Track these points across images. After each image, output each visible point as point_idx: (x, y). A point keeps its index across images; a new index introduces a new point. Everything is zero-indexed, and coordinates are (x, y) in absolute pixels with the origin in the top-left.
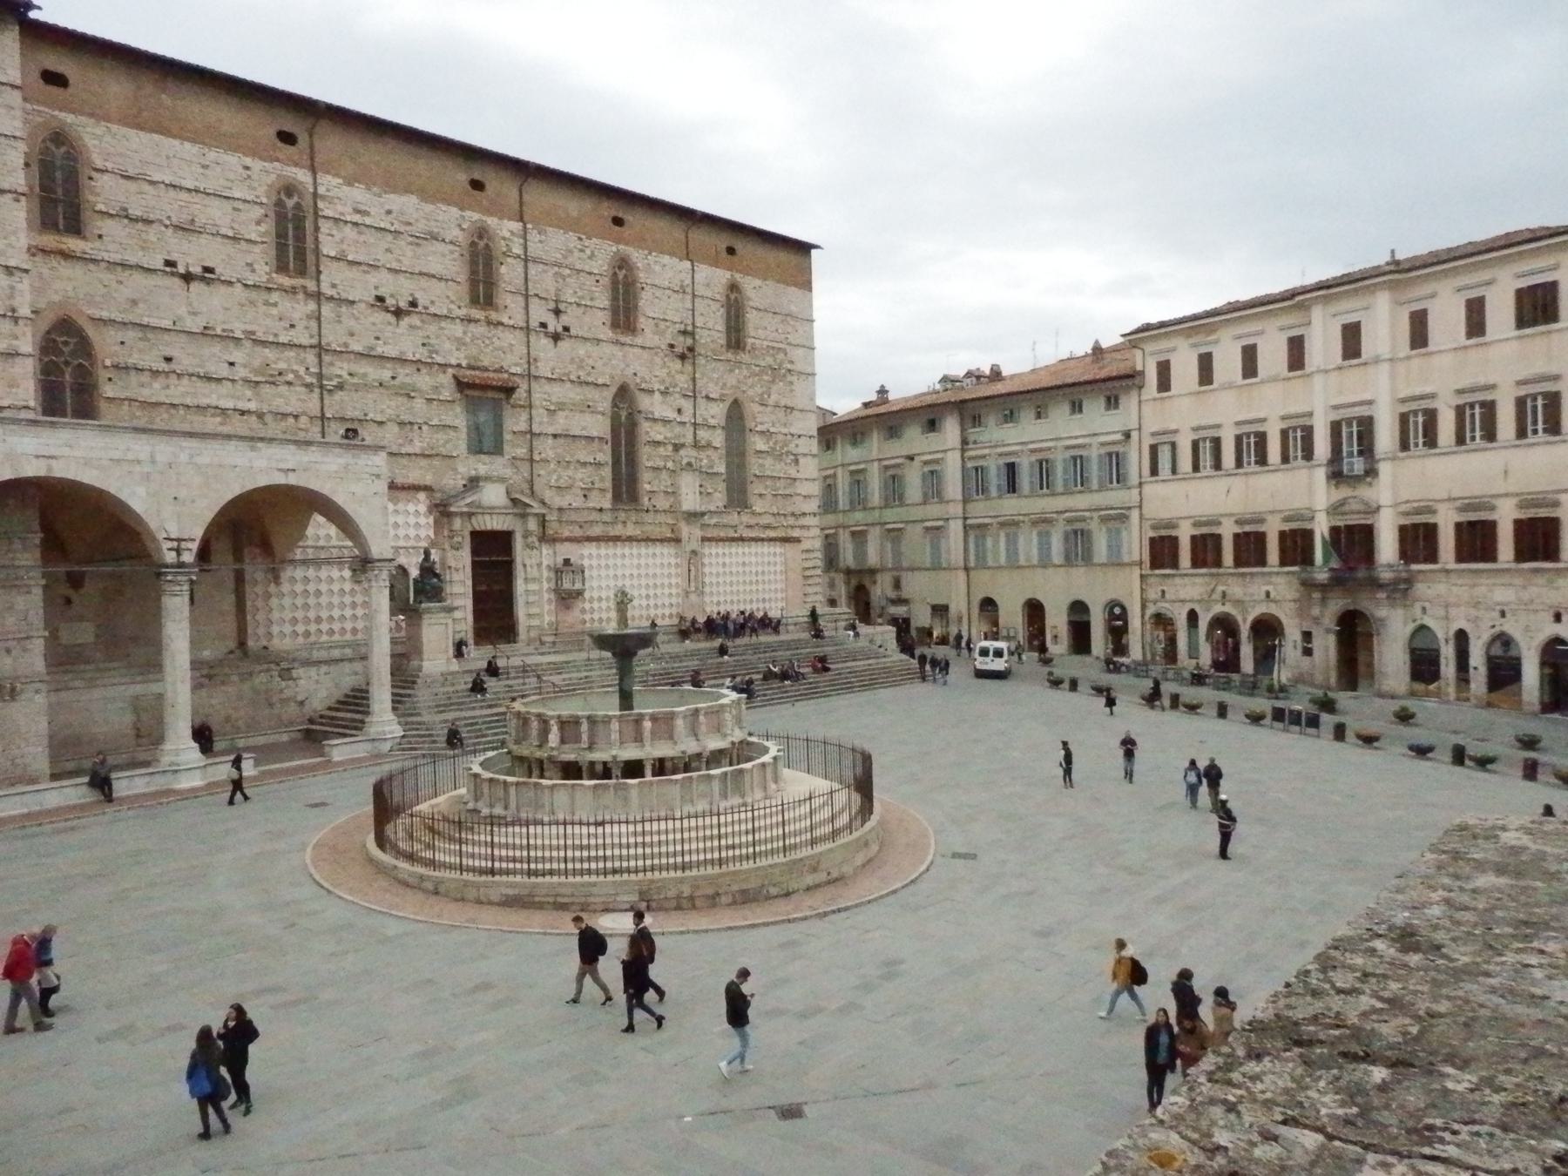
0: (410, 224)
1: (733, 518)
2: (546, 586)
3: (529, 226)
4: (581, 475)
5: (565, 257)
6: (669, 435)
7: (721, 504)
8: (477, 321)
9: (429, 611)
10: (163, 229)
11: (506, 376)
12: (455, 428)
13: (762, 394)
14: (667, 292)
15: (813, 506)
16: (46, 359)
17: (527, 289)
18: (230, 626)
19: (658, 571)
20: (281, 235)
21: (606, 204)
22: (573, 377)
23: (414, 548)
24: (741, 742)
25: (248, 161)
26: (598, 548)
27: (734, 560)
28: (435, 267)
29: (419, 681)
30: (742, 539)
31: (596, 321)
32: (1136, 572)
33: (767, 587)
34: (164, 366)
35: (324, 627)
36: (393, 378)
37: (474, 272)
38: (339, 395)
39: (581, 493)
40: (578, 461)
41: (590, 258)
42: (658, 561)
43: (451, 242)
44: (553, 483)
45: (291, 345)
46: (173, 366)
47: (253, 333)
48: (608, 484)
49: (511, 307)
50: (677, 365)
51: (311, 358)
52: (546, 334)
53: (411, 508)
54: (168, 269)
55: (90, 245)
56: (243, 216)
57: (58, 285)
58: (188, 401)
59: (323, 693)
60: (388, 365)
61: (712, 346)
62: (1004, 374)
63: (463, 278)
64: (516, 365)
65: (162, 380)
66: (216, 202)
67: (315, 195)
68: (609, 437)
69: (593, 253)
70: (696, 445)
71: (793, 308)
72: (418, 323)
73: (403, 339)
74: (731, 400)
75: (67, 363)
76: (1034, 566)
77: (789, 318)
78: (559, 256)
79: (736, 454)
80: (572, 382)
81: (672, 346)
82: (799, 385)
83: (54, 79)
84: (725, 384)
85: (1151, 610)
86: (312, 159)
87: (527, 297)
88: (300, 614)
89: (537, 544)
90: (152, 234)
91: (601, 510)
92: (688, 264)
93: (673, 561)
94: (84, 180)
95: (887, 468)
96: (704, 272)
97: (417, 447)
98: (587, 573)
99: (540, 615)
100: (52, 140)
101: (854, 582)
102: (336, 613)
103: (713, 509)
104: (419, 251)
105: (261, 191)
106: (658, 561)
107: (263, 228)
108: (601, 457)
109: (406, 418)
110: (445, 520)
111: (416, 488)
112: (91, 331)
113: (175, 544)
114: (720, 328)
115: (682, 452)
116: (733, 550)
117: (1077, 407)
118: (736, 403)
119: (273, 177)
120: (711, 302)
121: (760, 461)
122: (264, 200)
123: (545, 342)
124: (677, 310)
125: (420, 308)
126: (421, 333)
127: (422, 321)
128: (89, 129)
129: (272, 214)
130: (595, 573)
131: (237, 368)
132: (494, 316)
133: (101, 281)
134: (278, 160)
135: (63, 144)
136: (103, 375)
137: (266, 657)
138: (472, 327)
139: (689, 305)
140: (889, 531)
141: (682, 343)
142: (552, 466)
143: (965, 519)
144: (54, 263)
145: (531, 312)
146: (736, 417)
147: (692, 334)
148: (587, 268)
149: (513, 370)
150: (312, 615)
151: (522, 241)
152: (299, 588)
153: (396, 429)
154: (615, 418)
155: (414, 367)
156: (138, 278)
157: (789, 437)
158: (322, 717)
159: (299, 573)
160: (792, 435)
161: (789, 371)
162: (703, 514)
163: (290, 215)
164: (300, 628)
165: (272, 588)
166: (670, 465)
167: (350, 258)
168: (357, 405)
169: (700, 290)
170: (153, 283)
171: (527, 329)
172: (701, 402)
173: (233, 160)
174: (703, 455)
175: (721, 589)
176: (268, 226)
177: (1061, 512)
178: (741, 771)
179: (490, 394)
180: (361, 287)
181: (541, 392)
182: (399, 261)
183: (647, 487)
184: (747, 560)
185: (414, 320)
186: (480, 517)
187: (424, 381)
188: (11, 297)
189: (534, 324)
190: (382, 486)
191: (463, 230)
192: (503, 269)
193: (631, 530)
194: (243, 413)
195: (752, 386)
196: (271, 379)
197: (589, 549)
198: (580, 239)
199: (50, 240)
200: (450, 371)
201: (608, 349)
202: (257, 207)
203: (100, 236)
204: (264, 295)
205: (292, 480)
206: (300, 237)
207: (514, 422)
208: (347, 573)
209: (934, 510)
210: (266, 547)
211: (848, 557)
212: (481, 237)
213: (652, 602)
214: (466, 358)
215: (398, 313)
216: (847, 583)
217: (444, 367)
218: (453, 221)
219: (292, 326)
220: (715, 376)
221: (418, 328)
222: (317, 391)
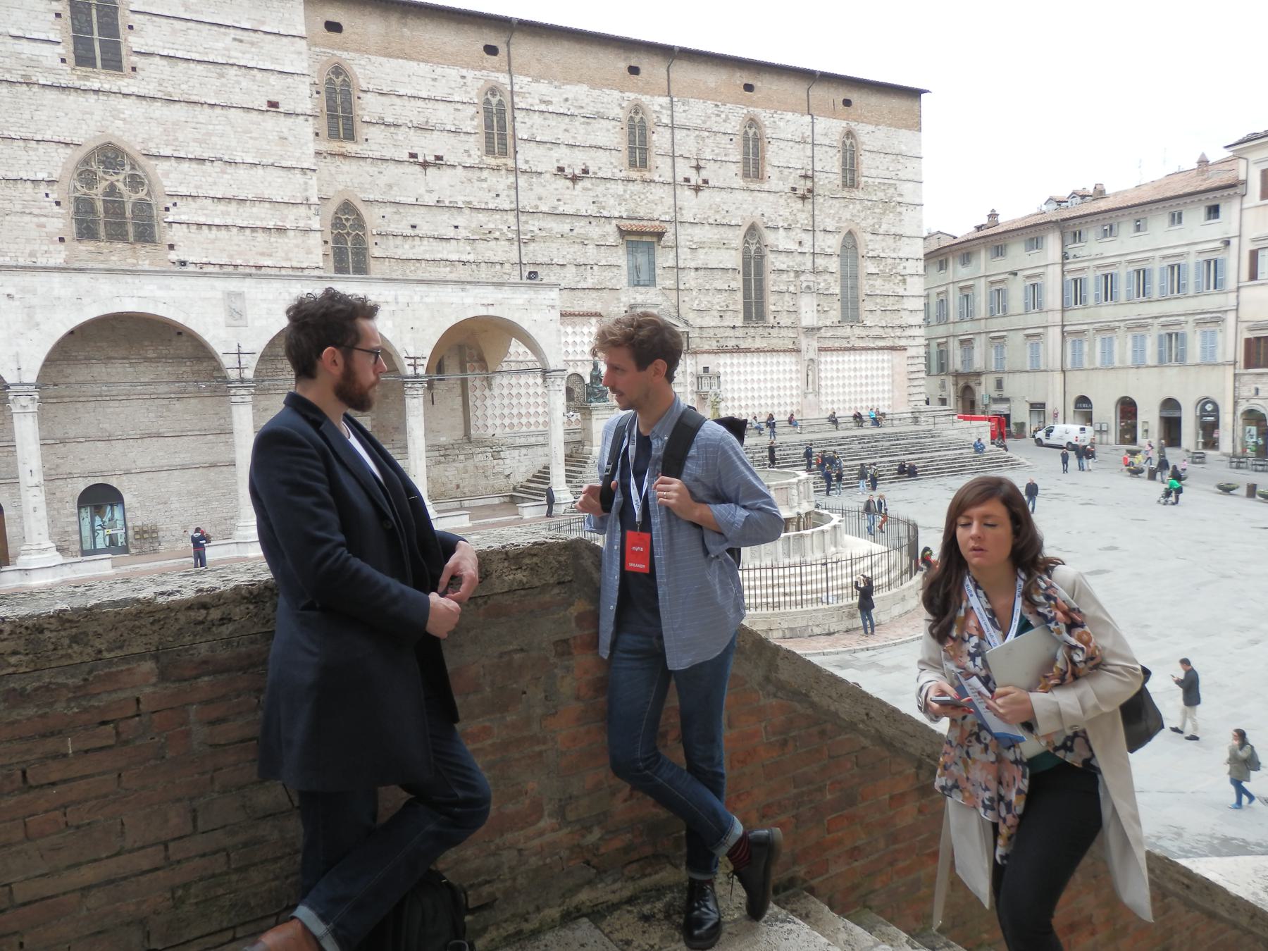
0: (582, 107)
1: (847, 331)
2: (689, 388)
3: (675, 99)
4: (719, 300)
5: (704, 122)
6: (791, 264)
7: (836, 320)
9: (596, 409)
10: (407, 130)
11: (657, 223)
13: (874, 225)
14: (791, 143)
15: (919, 318)
16: (335, 232)
18: (459, 420)
19: (781, 376)
20: (489, 126)
21: (738, 75)
22: (711, 221)
24: (808, 514)
25: (464, 72)
26: (732, 358)
27: (846, 366)
29: (589, 461)
30: (853, 349)
31: (730, 174)
32: (1230, 371)
33: (875, 388)
34: (410, 232)
35: (524, 421)
37: (632, 141)
38: (532, 246)
39: (717, 314)
41: (725, 121)
42: (781, 368)
44: (695, 307)
45: (496, 210)
46: (417, 232)
47: (470, 203)
48: (740, 307)
49: (661, 167)
50: (799, 205)
51: (511, 218)
53: (585, 330)
54: (412, 160)
55: (361, 147)
56: (460, 115)
57: (341, 178)
58: (428, 257)
59: (523, 469)
61: (829, 186)
62: (1107, 192)
63: (624, 146)
64: (666, 213)
65: (410, 241)
66: (441, 106)
67: (512, 92)
68: (741, 269)
69: (727, 116)
70: (815, 272)
71: (904, 148)
72: (589, 186)
73: (579, 199)
74: (844, 232)
75: (348, 234)
76: (1128, 367)
77: (899, 157)
78: (700, 122)
79: (850, 279)
81: (794, 189)
83: (334, 27)
84: (840, 218)
85: (1243, 406)
86: (509, 65)
87: (673, 157)
88: (506, 411)
90: (401, 134)
91: (734, 327)
93: (794, 368)
94: (354, 98)
95: (992, 283)
96: (822, 123)
97: (589, 283)
98: (722, 378)
100: (333, 73)
101: (961, 383)
102: (532, 411)
103: (829, 324)
104: (589, 128)
105: (473, 94)
106: (781, 368)
107: (475, 123)
108: (734, 285)
109: (582, 261)
112: (362, 209)
113: (413, 361)
114: (836, 171)
115: (802, 278)
116: (846, 358)
117: (1177, 218)
118: (850, 233)
119: (482, 82)
120: (829, 149)
121: (871, 282)
122: (476, 101)
123: (689, 193)
124: (799, 158)
125: (591, 174)
126: (591, 193)
127: (593, 184)
128: (356, 62)
129: (482, 111)
130: (729, 378)
131: (460, 229)
133: (368, 173)
134: (484, 68)
135: (341, 74)
136: (371, 241)
137: (481, 443)
140: (993, 338)
141: (803, 186)
142: (694, 293)
143: (1063, 326)
144: (338, 163)
145: (677, 170)
146: (850, 244)
147: (812, 178)
150: (515, 411)
152: (505, 392)
153: (573, 269)
154: (746, 251)
156: (392, 167)
157: (898, 261)
158: (522, 487)
159: (505, 380)
162: (819, 329)
163: (494, 111)
164: (507, 421)
165: (487, 392)
166: (792, 289)
167: (538, 139)
168: (546, 253)
169: (819, 139)
170: (402, 171)
171: (674, 184)
172: (819, 235)
173: (453, 73)
174: (820, 279)
175: (835, 391)
176: (479, 121)
177: (1156, 317)
178: (802, 536)
179: (645, 239)
180: (544, 160)
181: (686, 234)
183: (773, 308)
184: (858, 366)
185: (586, 183)
187: (595, 231)
188: (306, 190)
189: (680, 179)
190: (556, 315)
191: (623, 108)
192: (655, 137)
193: (759, 343)
194: (464, 263)
195: (864, 219)
196: (484, 237)
197: (725, 359)
198: (717, 106)
199: (335, 146)
200: (614, 222)
201: (739, 196)
202: (471, 106)
203: (367, 140)
204: (477, 173)
205: (492, 312)
206: (502, 127)
207: (664, 259)
208: (539, 381)
209: (1034, 319)
210: (482, 362)
211: (956, 362)
212: (636, 113)
213: (776, 401)
214: (626, 210)
215: (574, 179)
216: (956, 384)
218: (614, 101)
219: (498, 195)
220: (832, 211)
221: (590, 190)
222: (517, 243)
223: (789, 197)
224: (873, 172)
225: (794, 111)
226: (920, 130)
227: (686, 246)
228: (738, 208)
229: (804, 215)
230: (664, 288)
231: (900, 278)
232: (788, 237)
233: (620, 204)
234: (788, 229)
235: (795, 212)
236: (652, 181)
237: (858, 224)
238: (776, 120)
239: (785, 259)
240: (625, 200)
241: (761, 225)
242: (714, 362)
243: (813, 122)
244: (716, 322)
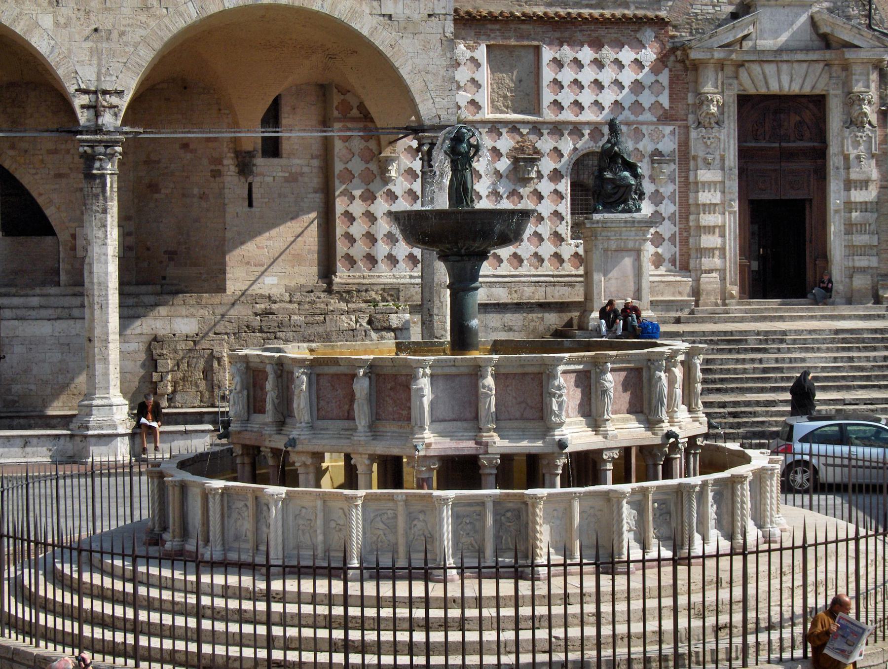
23: (628, 124)
53: (627, 55)
111: (639, 22)
186: (756, 69)
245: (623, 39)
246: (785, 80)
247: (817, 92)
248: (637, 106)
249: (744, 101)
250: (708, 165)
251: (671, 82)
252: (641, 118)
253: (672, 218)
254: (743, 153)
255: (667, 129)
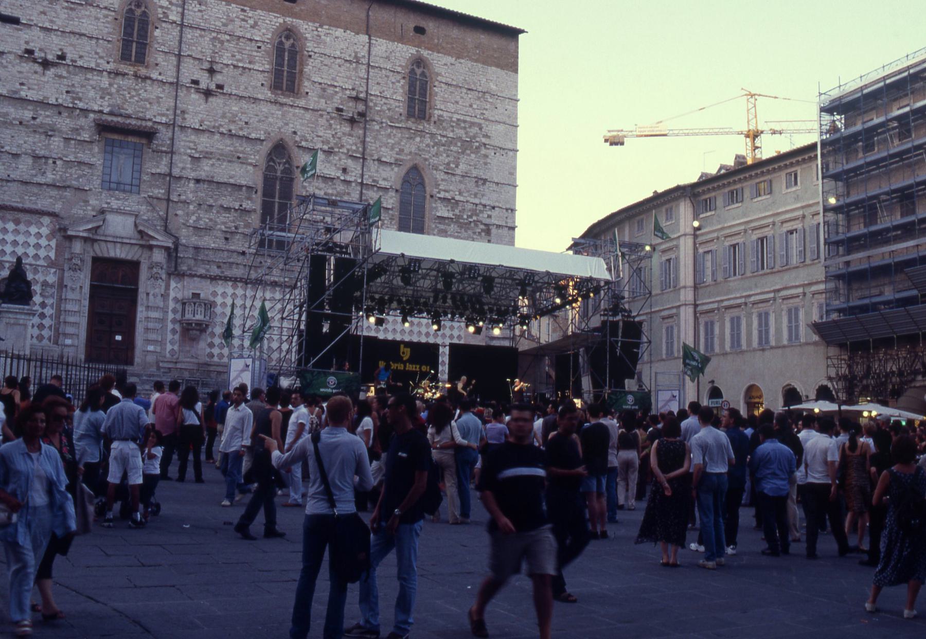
6: (330, 191)
8: (124, 75)
11: (150, 124)
12: (91, 166)
13: (448, 164)
14: (338, 61)
17: (180, 51)
22: (221, 130)
23: (31, 265)
28: (87, 26)
36: (34, 118)
40: (222, 206)
41: (253, 27)
43: (106, 8)
52: (198, 91)
53: (33, 230)
60: (30, 107)
63: (114, 37)
64: (163, 115)
68: (260, 187)
69: (256, 24)
72: (65, 74)
74: (408, 165)
78: (219, 24)
80: (222, 134)
81: (339, 110)
82: (495, 160)
84: (402, 151)
87: (179, 56)
89: (164, 276)
91: (243, 253)
92: (364, 38)
96: (382, 46)
97: (50, 177)
99: (162, 343)
104: (73, 14)
108: (247, 205)
110: (67, 244)
114: (401, 98)
118: (415, 169)
121: (442, 227)
125: (68, 61)
126: (65, 81)
127: (68, 72)
132: (143, 71)
138: (119, 80)
139: (363, 74)
141: (351, 109)
142: (191, 207)
143: (696, 306)
147: (365, 101)
148: (248, 36)
149: (158, 119)
151: (180, 10)
153: (30, 161)
154: (269, 168)
155: (56, 110)
157: (480, 207)
160: (485, 206)
161: (485, 144)
171: (176, 85)
172: (372, 166)
181: (184, 142)
182: (51, 21)
186: (103, 244)
187: (64, 123)
195: (436, 155)
198: (243, 10)
200: (92, 115)
201: (265, 108)
217: (85, 112)
221: (64, 77)
223: (332, 118)
224: (451, 107)
225: (346, 29)
226: (516, 71)
227: (185, 154)
228: (259, 121)
229: (351, 140)
230: (150, 197)
231: (482, 227)
232: (329, 162)
233: (102, 98)
234: (329, 153)
235: (339, 134)
236: (146, 78)
237: (426, 160)
238: (322, 34)
239: (322, 185)
240: (110, 94)
241: (291, 144)
242: (206, 290)
243: (370, 43)
244: (220, 244)
245: (33, 221)
246: (118, 251)
247: (135, 259)
248: (36, 256)
249: (96, 260)
250: (73, 290)
251: (57, 246)
252: (38, 263)
253: (51, 317)
254: (93, 287)
255: (53, 270)
